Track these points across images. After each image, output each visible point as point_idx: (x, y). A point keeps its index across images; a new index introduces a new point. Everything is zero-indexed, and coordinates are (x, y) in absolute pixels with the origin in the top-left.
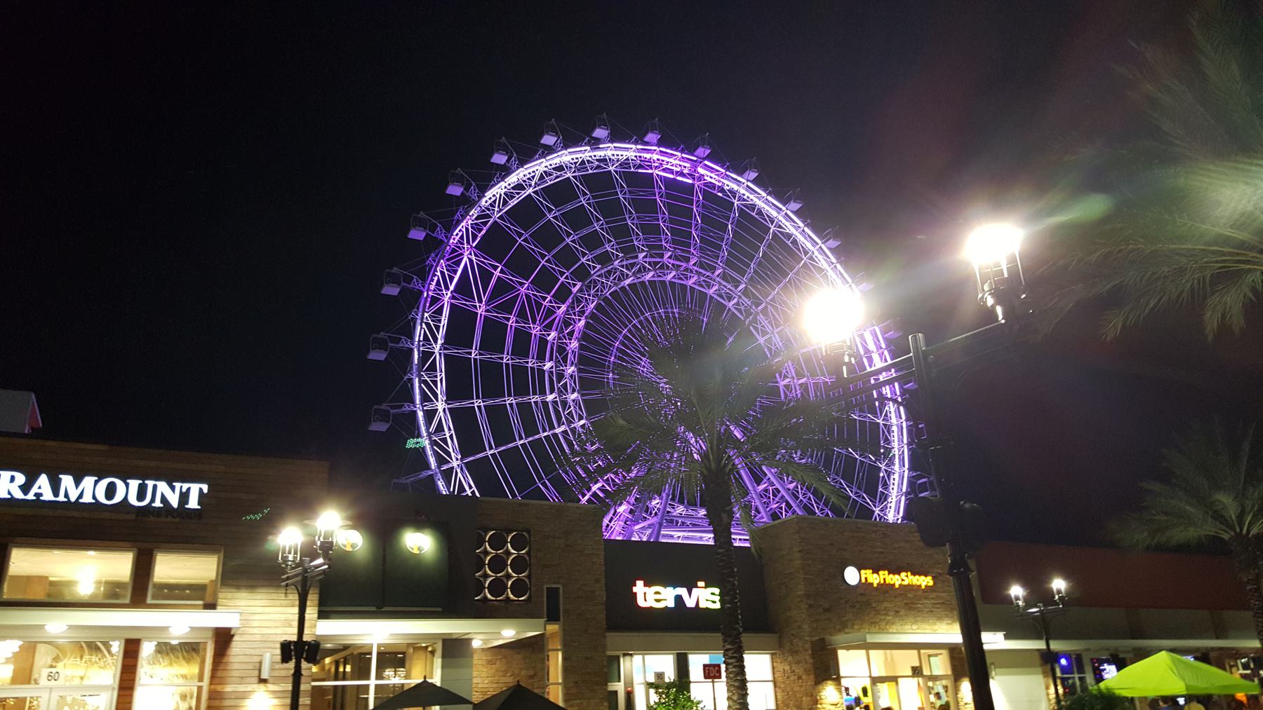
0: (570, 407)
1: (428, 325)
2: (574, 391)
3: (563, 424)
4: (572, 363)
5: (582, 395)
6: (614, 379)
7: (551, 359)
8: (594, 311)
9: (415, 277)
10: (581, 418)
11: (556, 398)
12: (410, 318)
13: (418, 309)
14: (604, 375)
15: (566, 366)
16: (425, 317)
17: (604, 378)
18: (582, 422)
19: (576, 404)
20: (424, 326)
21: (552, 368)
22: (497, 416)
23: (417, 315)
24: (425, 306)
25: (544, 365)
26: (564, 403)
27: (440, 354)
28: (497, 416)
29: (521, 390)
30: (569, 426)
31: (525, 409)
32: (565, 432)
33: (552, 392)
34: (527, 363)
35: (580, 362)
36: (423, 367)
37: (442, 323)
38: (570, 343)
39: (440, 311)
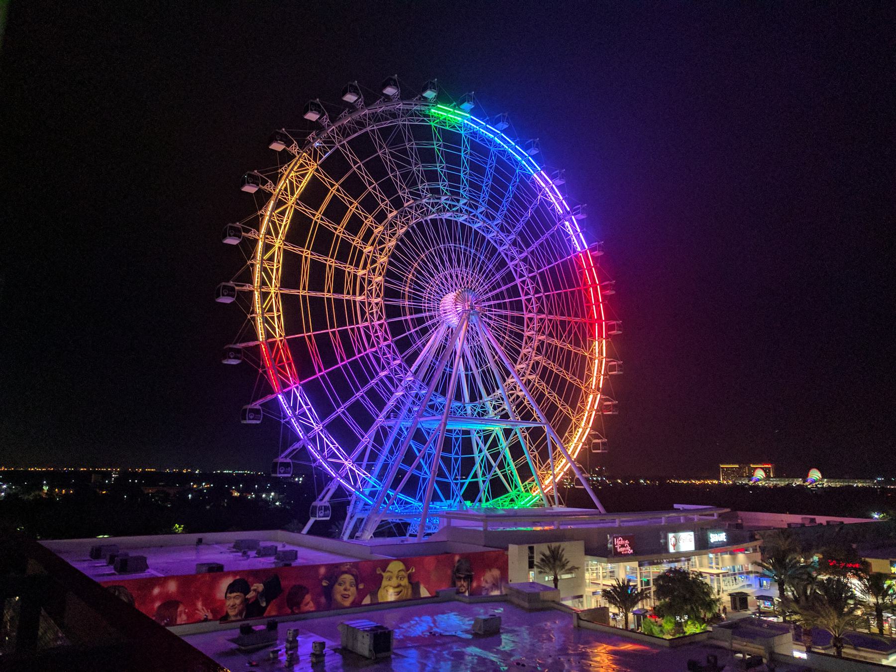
0: (372, 285)
1: (291, 183)
2: (380, 274)
3: (364, 295)
4: (387, 254)
5: (386, 281)
6: (412, 280)
7: (372, 245)
8: (414, 225)
9: (295, 142)
10: (378, 296)
11: (365, 275)
12: (279, 171)
13: (289, 166)
14: (406, 273)
15: (380, 254)
16: (291, 175)
17: (404, 276)
18: (379, 299)
19: (378, 286)
20: (287, 181)
21: (370, 252)
22: (318, 270)
23: (286, 170)
24: (293, 167)
25: (365, 248)
26: (370, 282)
27: (292, 207)
28: (318, 270)
29: (342, 257)
30: (368, 298)
31: (339, 274)
32: (363, 303)
33: (364, 268)
34: (353, 240)
35: (393, 256)
36: (276, 210)
37: (302, 186)
38: (390, 240)
39: (303, 176)
